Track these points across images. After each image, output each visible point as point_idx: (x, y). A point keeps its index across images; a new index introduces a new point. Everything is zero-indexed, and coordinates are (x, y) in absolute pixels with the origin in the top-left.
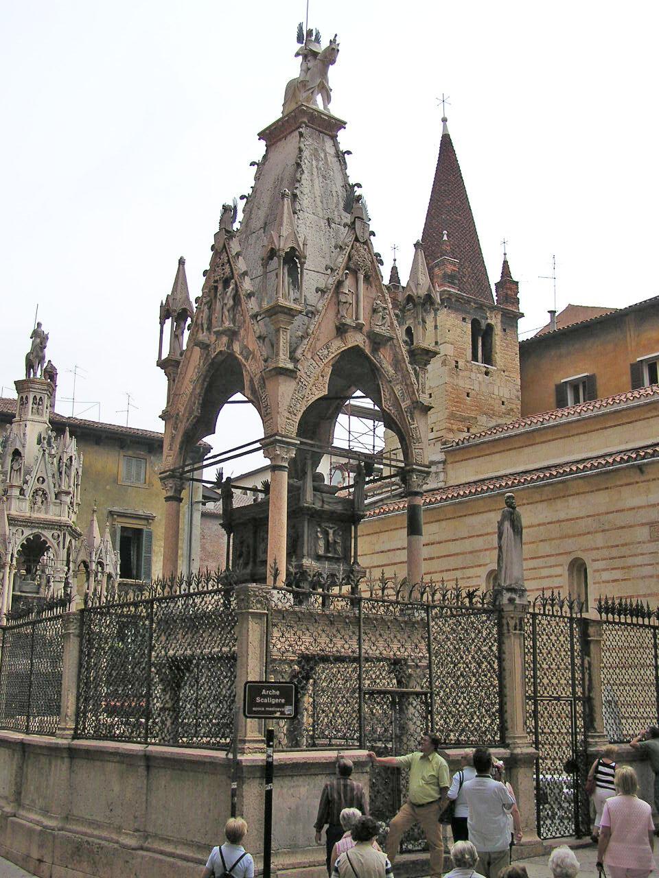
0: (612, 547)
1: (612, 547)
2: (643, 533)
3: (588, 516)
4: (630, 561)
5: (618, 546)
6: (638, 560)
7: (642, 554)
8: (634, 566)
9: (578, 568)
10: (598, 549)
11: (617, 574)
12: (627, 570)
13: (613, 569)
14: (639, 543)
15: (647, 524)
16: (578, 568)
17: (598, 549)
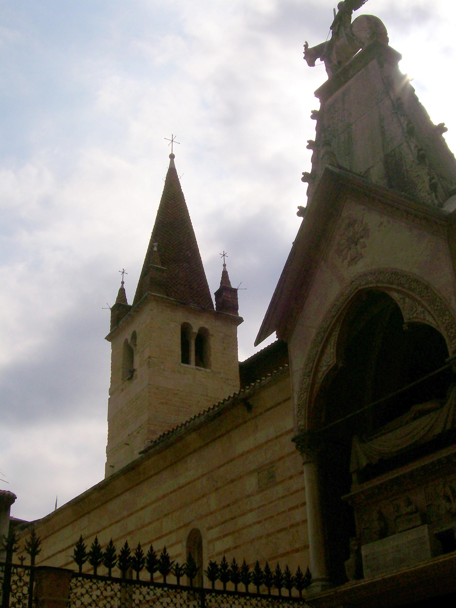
0: (224, 507)
1: (224, 507)
2: (251, 483)
3: (203, 476)
4: (241, 522)
5: (228, 505)
6: (250, 518)
7: (251, 510)
8: (243, 529)
9: (195, 541)
10: (212, 513)
11: (228, 542)
12: (237, 535)
13: (225, 536)
14: (249, 496)
15: (254, 471)
16: (195, 541)
17: (212, 513)
